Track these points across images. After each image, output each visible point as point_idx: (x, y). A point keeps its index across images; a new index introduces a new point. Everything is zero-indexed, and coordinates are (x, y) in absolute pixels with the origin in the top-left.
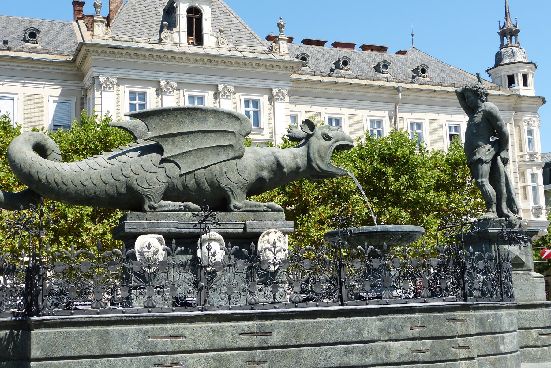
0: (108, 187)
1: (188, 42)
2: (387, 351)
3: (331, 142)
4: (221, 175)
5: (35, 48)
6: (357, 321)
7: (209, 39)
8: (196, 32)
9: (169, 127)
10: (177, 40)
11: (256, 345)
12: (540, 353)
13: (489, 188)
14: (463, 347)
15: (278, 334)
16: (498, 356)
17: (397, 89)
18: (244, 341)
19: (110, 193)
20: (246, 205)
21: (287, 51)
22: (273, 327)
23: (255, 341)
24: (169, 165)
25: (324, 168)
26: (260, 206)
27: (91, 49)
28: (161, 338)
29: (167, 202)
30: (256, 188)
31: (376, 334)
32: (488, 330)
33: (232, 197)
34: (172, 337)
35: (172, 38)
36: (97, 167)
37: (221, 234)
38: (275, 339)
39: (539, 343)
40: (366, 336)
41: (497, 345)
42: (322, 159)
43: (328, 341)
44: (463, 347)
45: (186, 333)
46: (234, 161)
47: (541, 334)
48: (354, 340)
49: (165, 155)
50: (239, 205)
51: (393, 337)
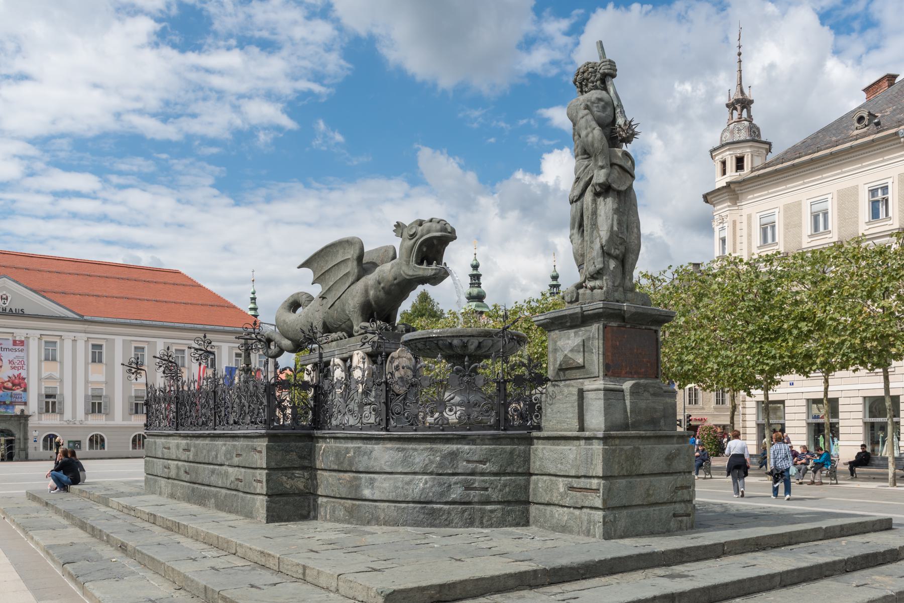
12: (566, 518)
16: (357, 503)
25: (411, 273)
32: (346, 466)
39: (567, 501)
41: (358, 487)
47: (572, 488)
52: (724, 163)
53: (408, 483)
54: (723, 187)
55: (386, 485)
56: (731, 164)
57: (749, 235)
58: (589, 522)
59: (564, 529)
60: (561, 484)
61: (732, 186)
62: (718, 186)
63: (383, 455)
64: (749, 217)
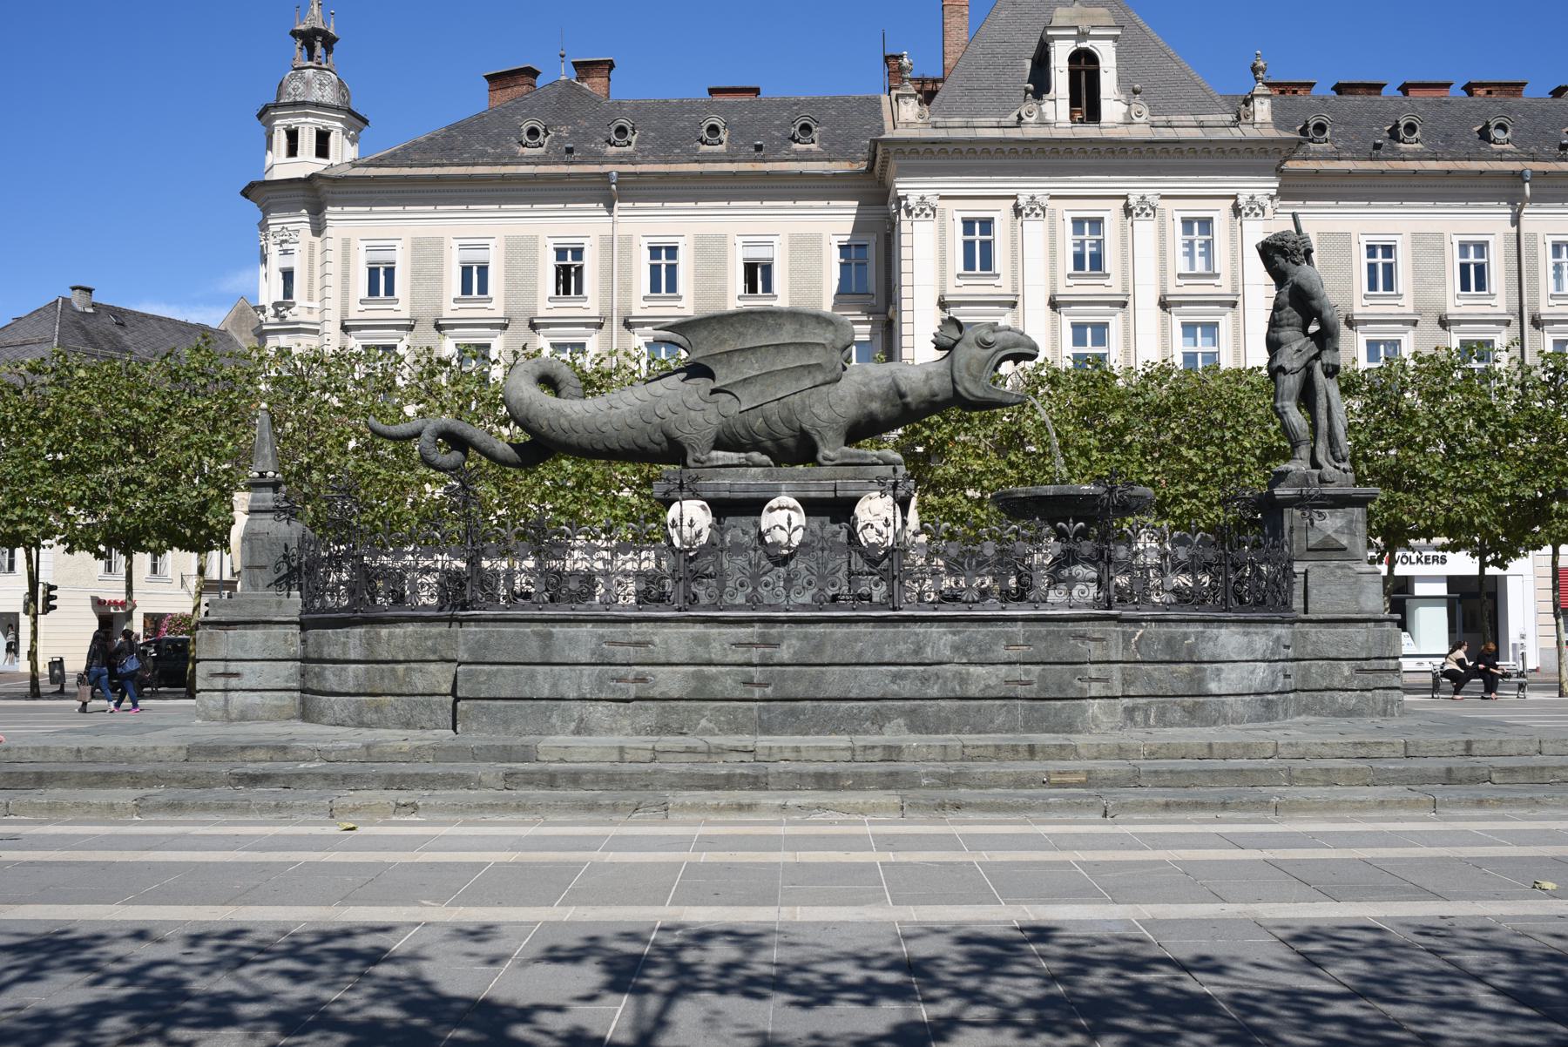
0: (635, 433)
1: (1072, 117)
2: (963, 680)
3: (991, 351)
4: (803, 410)
5: (809, 151)
6: (917, 634)
7: (1112, 107)
8: (1086, 99)
9: (723, 342)
10: (1050, 117)
11: (755, 660)
13: (1297, 418)
14: (1097, 680)
15: (789, 647)
16: (1201, 700)
17: (1519, 176)
18: (739, 656)
19: (640, 442)
20: (844, 455)
21: (1269, 119)
22: (782, 637)
23: (755, 655)
24: (723, 397)
25: (980, 393)
26: (866, 456)
27: (892, 149)
28: (622, 644)
29: (721, 454)
30: (862, 429)
31: (947, 653)
32: (1183, 655)
33: (820, 444)
34: (637, 644)
35: (1041, 113)
36: (621, 405)
37: (799, 500)
38: (784, 653)
40: (929, 654)
41: (1201, 681)
42: (976, 379)
43: (865, 659)
44: (1097, 680)
45: (656, 640)
46: (824, 389)
47: (1362, 670)
48: (909, 660)
49: (718, 385)
50: (832, 455)
51: (974, 658)
52: (292, 136)
53: (1252, 672)
54: (299, 180)
55: (1233, 676)
56: (307, 142)
57: (346, 276)
58: (1386, 702)
59: (1350, 713)
60: (1346, 668)
61: (319, 183)
62: (278, 174)
63: (1229, 639)
64: (346, 243)
